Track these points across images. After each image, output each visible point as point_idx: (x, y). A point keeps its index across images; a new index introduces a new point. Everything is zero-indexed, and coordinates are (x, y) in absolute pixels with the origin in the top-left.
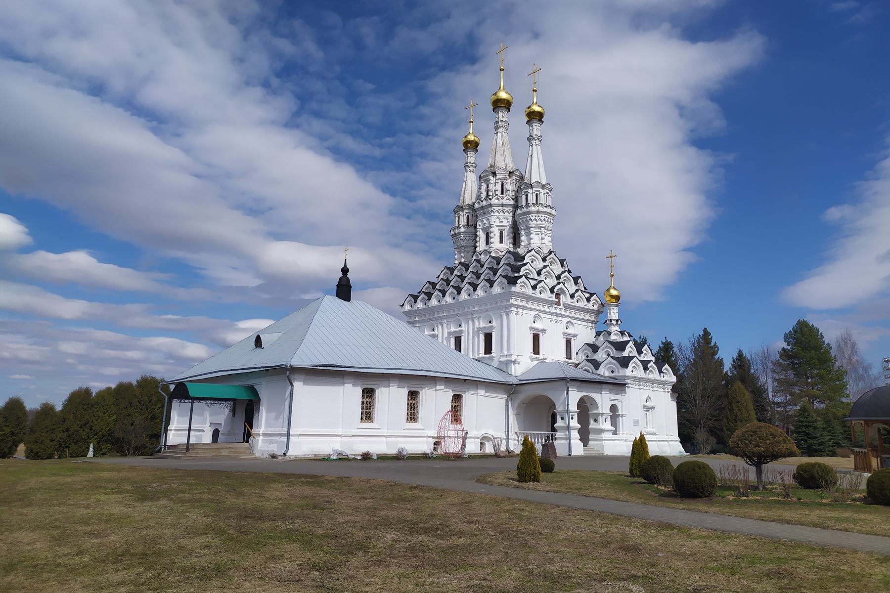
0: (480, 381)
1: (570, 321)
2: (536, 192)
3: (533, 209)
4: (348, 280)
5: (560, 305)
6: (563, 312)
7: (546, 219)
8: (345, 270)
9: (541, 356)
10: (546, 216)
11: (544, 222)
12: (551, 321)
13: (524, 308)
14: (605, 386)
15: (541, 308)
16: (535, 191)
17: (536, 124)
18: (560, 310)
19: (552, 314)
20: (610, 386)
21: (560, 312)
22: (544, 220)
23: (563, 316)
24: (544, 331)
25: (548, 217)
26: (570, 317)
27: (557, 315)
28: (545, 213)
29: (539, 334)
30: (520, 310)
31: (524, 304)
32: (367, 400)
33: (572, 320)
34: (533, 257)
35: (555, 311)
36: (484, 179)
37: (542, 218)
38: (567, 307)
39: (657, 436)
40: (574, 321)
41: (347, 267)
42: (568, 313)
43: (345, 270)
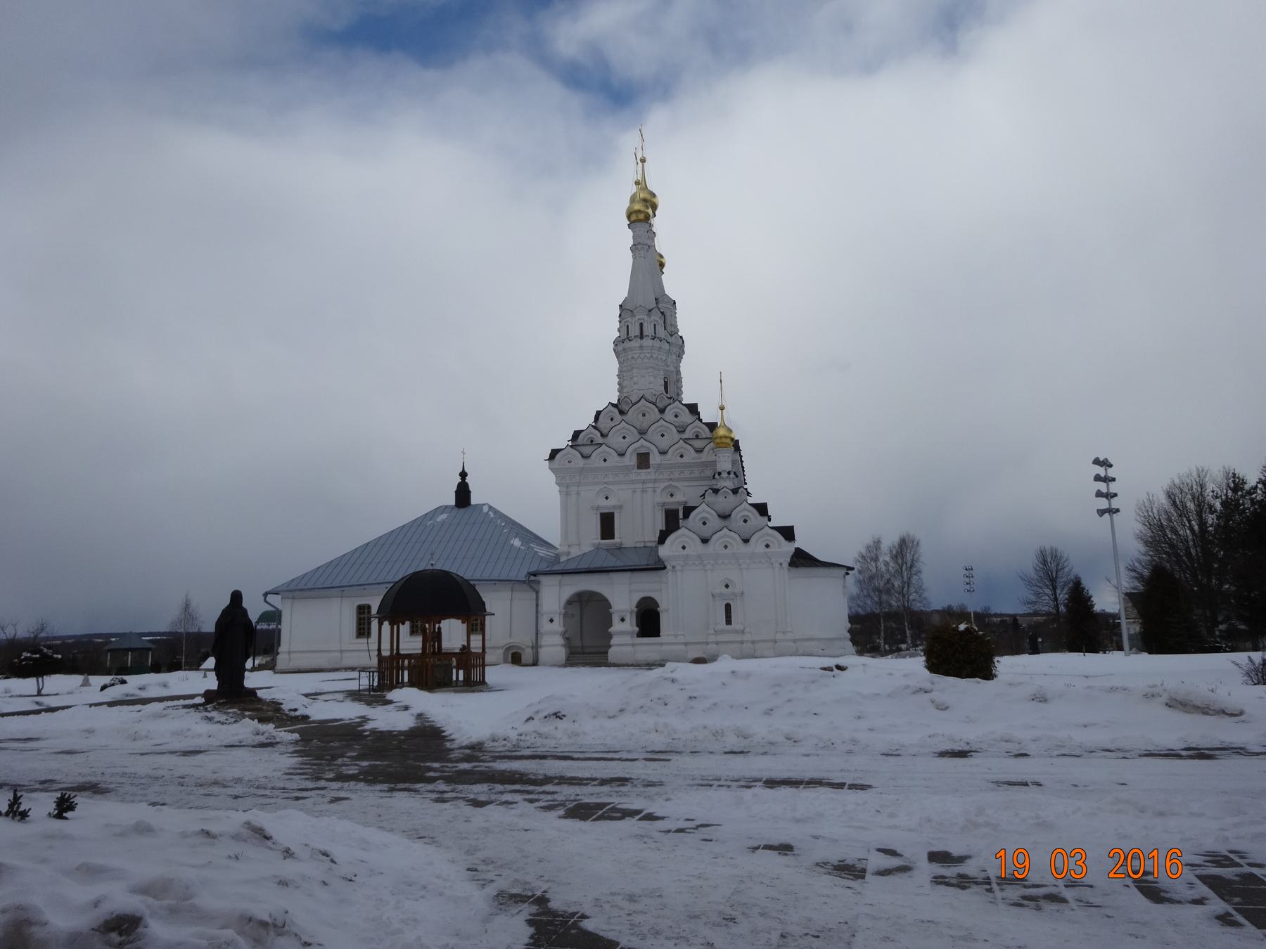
4: (467, 485)
5: (649, 468)
7: (636, 356)
8: (463, 475)
9: (617, 540)
12: (634, 492)
13: (579, 484)
14: (613, 575)
19: (632, 482)
20: (628, 574)
23: (655, 481)
24: (621, 507)
26: (671, 479)
33: (675, 484)
34: (611, 414)
38: (659, 467)
40: (675, 484)
41: (466, 470)
43: (463, 475)
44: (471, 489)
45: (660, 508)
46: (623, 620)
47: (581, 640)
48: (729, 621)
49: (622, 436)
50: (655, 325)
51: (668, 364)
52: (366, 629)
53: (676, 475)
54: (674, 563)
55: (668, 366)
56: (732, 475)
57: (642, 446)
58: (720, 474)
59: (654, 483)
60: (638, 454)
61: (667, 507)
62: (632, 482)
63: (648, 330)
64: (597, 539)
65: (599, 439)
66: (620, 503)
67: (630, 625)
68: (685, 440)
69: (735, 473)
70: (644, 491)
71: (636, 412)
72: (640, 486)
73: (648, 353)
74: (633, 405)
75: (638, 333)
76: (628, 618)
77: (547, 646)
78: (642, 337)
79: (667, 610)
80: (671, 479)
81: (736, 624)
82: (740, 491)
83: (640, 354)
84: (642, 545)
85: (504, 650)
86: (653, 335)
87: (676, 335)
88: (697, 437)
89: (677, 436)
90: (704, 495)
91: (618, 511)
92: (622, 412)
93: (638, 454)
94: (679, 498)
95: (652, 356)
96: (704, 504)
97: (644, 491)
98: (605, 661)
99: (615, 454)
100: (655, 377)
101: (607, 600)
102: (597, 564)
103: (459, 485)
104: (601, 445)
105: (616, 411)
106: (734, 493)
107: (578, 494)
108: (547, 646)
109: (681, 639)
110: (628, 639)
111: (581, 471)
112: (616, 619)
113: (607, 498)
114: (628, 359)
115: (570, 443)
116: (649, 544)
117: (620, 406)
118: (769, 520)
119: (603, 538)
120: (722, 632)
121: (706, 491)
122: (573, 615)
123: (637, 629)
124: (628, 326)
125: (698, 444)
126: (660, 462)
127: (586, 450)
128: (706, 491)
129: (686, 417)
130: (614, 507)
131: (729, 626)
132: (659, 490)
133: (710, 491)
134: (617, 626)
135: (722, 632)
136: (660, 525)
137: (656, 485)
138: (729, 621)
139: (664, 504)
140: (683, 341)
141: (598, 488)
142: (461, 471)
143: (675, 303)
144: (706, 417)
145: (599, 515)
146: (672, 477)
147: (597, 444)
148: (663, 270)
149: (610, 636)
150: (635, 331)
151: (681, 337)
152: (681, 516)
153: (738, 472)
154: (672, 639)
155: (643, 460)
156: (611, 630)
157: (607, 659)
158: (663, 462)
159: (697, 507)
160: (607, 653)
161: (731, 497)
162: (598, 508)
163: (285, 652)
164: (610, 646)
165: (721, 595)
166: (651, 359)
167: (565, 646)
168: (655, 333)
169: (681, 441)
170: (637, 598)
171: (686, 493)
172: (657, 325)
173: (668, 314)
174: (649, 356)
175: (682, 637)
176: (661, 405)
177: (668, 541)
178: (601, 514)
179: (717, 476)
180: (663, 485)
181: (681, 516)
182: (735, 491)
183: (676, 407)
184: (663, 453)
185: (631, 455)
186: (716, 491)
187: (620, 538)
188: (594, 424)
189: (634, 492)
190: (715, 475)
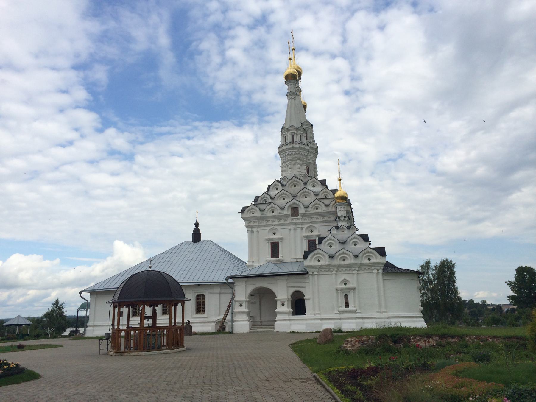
0: (210, 284)
1: (311, 225)
2: (285, 136)
3: (291, 146)
4: (199, 230)
5: (298, 216)
6: (300, 221)
8: (197, 224)
9: (280, 258)
10: (290, 151)
11: (289, 157)
12: (290, 230)
13: (259, 226)
14: (276, 277)
15: (276, 222)
16: (291, 133)
17: (291, 83)
18: (295, 220)
20: (286, 277)
21: (298, 221)
22: (288, 154)
23: (302, 223)
24: (282, 239)
25: (292, 151)
26: (311, 222)
27: (295, 224)
28: (288, 149)
29: (278, 242)
30: (255, 229)
31: (257, 224)
32: (200, 301)
34: (277, 186)
35: (292, 222)
36: (284, 134)
37: (287, 154)
38: (304, 216)
39: (358, 314)
41: (198, 222)
42: (308, 220)
43: (197, 224)
44: (201, 232)
45: (305, 239)
46: (283, 305)
47: (260, 318)
48: (347, 306)
49: (283, 198)
50: (301, 136)
51: (309, 159)
52: (137, 312)
53: (314, 220)
54: (313, 270)
55: (309, 160)
56: (347, 218)
57: (294, 203)
58: (339, 218)
59: (302, 224)
60: (292, 208)
61: (309, 238)
62: (289, 224)
63: (297, 139)
64: (269, 257)
65: (270, 201)
66: (282, 237)
67: (287, 308)
68: (319, 200)
69: (348, 217)
70: (296, 229)
71: (291, 185)
72: (294, 226)
73: (297, 151)
74: (289, 180)
75: (291, 141)
76: (286, 304)
77: (238, 321)
78: (293, 142)
79: (309, 299)
80: (311, 222)
81: (351, 308)
82: (351, 227)
83: (293, 152)
84: (295, 260)
85: (215, 324)
86: (300, 141)
87: (313, 142)
88: (326, 198)
89: (314, 198)
90: (330, 230)
91: (281, 241)
92: (282, 185)
93: (292, 208)
94: (316, 233)
95: (299, 153)
96: (330, 235)
97: (296, 229)
98: (273, 330)
99: (278, 208)
100: (301, 165)
101: (274, 293)
102: (267, 271)
103: (195, 230)
104: (271, 203)
105: (279, 184)
106: (348, 229)
107: (258, 232)
108: (238, 321)
109: (318, 316)
110: (286, 317)
111: (260, 218)
112: (279, 304)
113: (274, 234)
114: (286, 155)
115: (253, 203)
116: (299, 260)
117: (281, 182)
118: (370, 244)
119: (272, 257)
120: (343, 312)
121: (331, 228)
122: (255, 303)
123: (292, 310)
124: (285, 137)
125: (327, 202)
126: (304, 213)
127: (262, 207)
128: (331, 228)
129: (318, 188)
130: (279, 239)
131: (347, 309)
132: (304, 229)
133: (334, 228)
134: (280, 309)
135: (343, 312)
136: (305, 248)
137: (303, 226)
138: (347, 306)
139: (307, 237)
140: (317, 147)
141: (269, 228)
142: (196, 222)
143: (312, 125)
144: (330, 188)
145: (270, 244)
146: (312, 221)
147: (268, 203)
148: (306, 110)
149: (275, 315)
150: (289, 139)
151: (316, 144)
152: (317, 243)
153: (350, 217)
154: (313, 317)
155: (295, 211)
156: (276, 310)
157: (274, 329)
158: (306, 212)
159: (325, 237)
160: (274, 325)
161: (346, 231)
162: (269, 240)
163: (90, 326)
164: (276, 321)
165: (342, 289)
166: (299, 155)
167: (249, 321)
168: (301, 140)
169: (317, 200)
170: (292, 291)
171: (320, 230)
172: (302, 136)
173: (308, 132)
174: (297, 153)
175: (319, 315)
176: (305, 180)
177: (309, 257)
178: (271, 243)
179: (338, 219)
180: (306, 226)
181: (317, 243)
182: (349, 228)
183: (314, 181)
184: (306, 207)
185: (288, 207)
186: (337, 228)
187: (282, 257)
188: (267, 192)
189: (290, 230)
190: (336, 218)
